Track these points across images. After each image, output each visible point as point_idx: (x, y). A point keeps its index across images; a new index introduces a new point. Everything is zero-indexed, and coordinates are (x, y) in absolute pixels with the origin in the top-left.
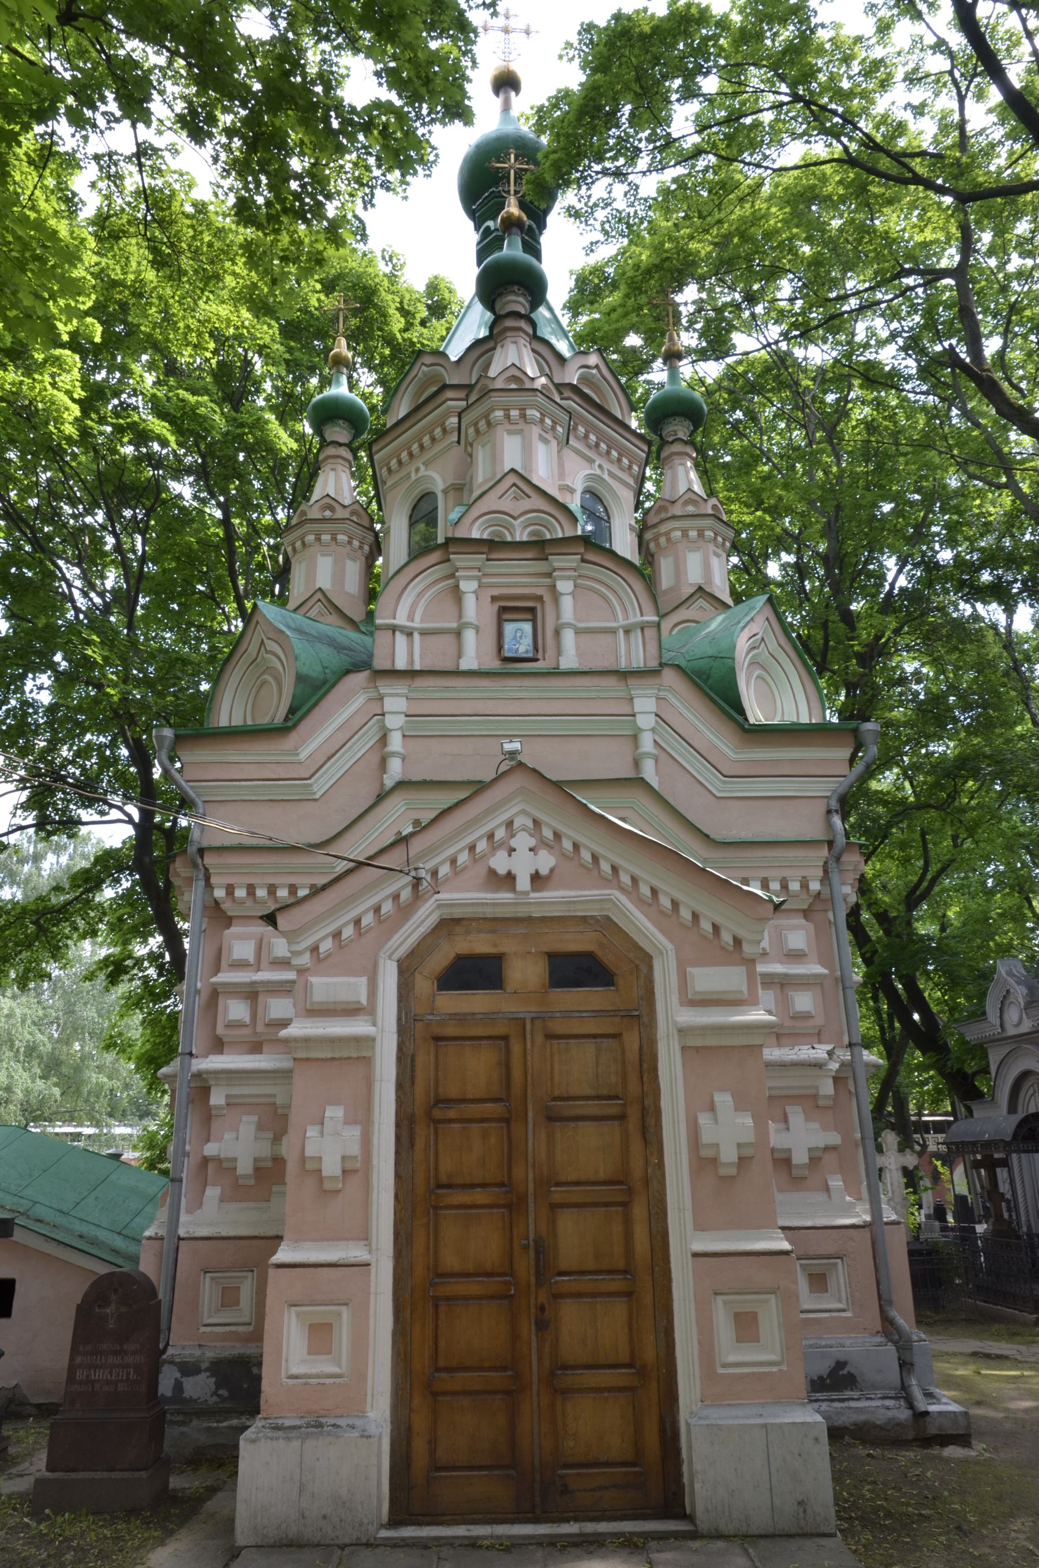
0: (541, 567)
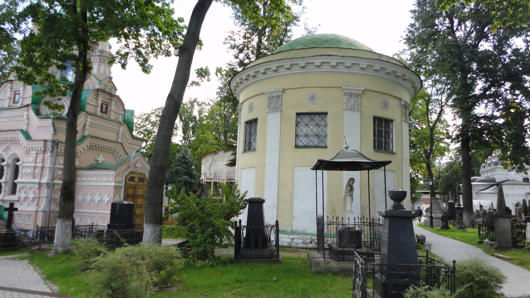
0: (110, 97)
